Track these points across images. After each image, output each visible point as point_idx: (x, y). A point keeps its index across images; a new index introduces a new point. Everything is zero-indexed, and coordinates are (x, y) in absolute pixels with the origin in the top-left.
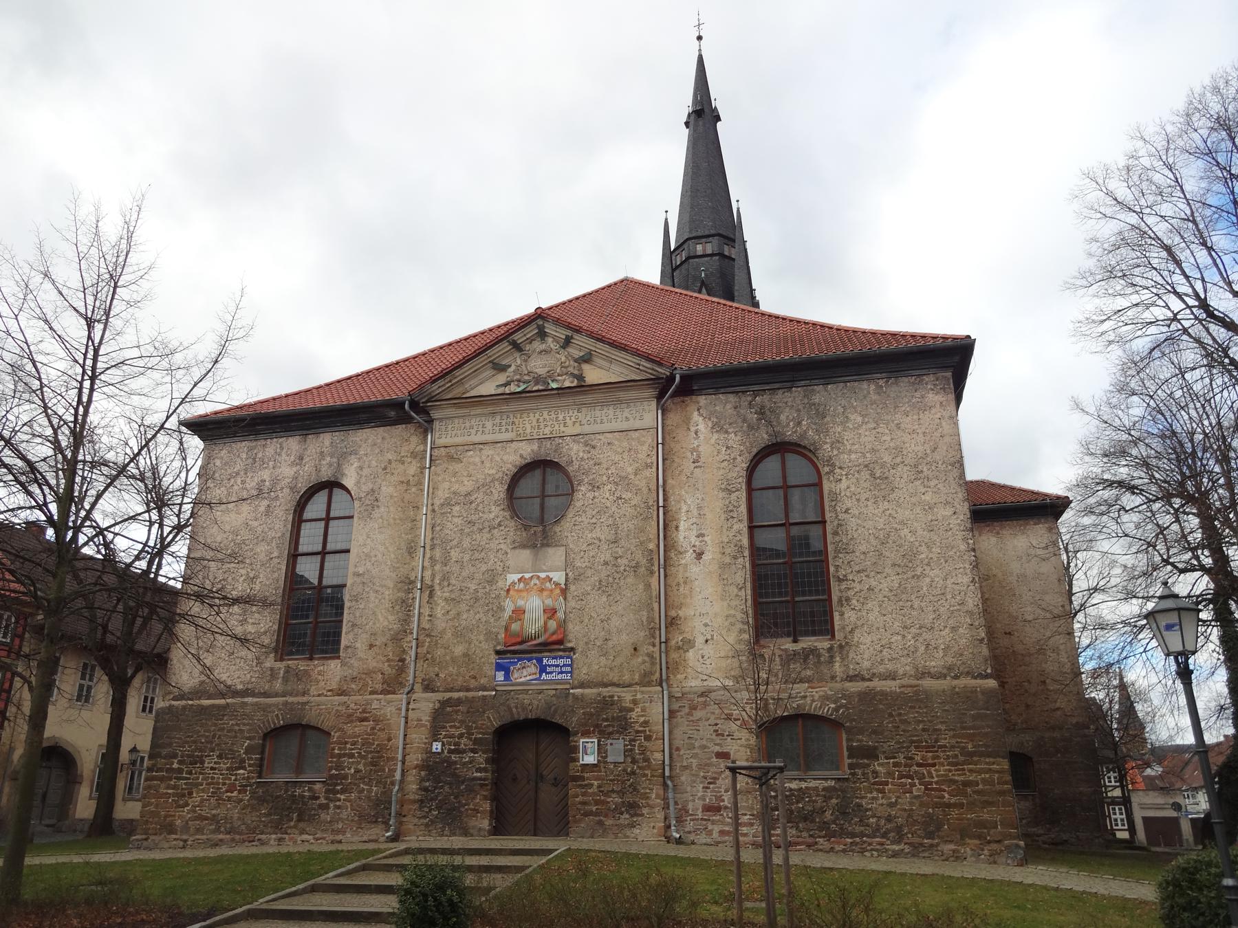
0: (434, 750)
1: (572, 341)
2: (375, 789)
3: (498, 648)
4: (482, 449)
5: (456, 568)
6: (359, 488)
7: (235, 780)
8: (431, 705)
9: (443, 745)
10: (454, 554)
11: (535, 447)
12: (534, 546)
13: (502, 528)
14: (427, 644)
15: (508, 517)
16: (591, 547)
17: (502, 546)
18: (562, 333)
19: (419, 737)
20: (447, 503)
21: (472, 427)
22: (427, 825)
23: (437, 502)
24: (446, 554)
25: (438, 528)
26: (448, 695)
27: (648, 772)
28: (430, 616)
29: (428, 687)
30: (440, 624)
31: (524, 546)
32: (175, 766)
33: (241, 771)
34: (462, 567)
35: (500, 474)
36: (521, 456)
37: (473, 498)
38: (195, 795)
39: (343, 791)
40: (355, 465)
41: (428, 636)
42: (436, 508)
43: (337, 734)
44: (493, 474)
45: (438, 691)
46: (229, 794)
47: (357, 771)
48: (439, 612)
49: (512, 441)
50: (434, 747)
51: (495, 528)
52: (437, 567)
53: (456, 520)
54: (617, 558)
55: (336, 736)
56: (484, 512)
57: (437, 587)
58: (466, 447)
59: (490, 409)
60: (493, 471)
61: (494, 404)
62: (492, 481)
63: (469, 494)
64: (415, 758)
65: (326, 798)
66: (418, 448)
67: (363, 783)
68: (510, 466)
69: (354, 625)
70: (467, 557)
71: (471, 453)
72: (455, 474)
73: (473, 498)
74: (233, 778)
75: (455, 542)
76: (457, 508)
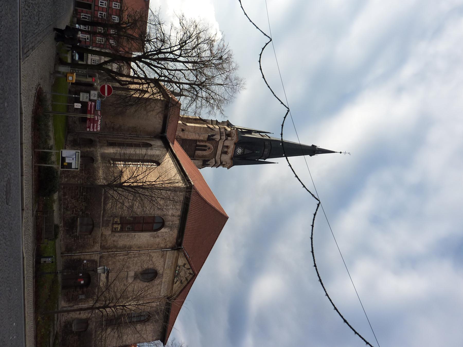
0: (84, 261)
1: (186, 281)
2: (75, 247)
3: (110, 271)
4: (163, 262)
5: (132, 260)
6: (160, 233)
7: (79, 212)
8: (96, 259)
9: (85, 263)
10: (136, 259)
11: (161, 273)
12: (135, 276)
13: (141, 269)
14: (113, 256)
15: (143, 270)
16: (132, 286)
17: (136, 269)
18: (189, 279)
19: (88, 257)
20: (150, 256)
21: (170, 259)
22: (65, 262)
23: (151, 254)
24: (137, 257)
25: (144, 254)
26: (98, 262)
27: (77, 303)
28: (120, 256)
29: (101, 257)
30: (117, 258)
31: (135, 274)
32: (84, 194)
33: (81, 213)
34: (132, 261)
35: (155, 266)
36: (159, 271)
37: (150, 261)
38: (75, 201)
39: (74, 239)
40: (167, 231)
41: (115, 256)
42: (149, 254)
43: (90, 236)
44: (156, 265)
45: (100, 260)
46: (75, 210)
47: (80, 243)
48: (121, 257)
49: (164, 268)
50: (85, 261)
51: (141, 267)
52: (133, 256)
53: (145, 258)
54: (129, 292)
55: (90, 236)
56: (146, 264)
57: (128, 256)
58: (165, 258)
59: (174, 263)
60: (157, 265)
61: (175, 264)
62: (154, 265)
63: (152, 260)
64: (82, 257)
65: (73, 236)
66: (168, 246)
67: (77, 244)
68: (157, 268)
69: (120, 236)
70: (135, 262)
71: (163, 260)
72: (158, 257)
73: (150, 261)
74: (79, 211)
75: (139, 259)
76: (148, 258)
